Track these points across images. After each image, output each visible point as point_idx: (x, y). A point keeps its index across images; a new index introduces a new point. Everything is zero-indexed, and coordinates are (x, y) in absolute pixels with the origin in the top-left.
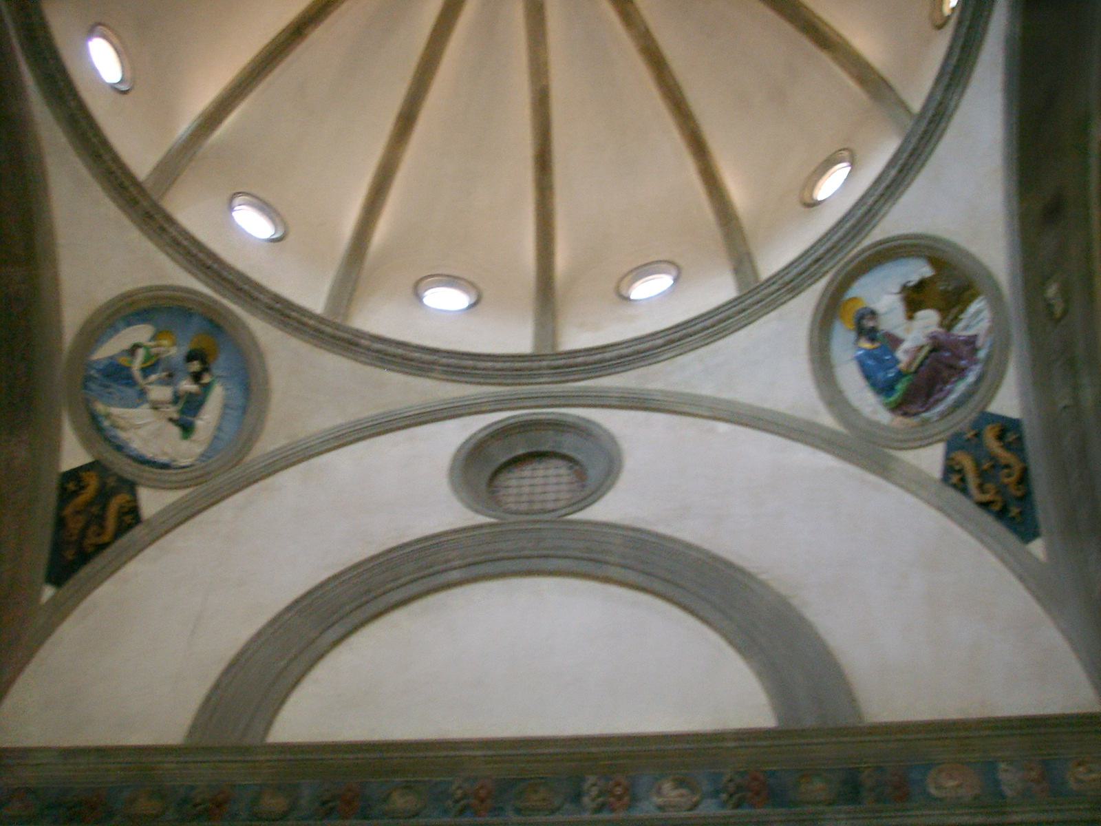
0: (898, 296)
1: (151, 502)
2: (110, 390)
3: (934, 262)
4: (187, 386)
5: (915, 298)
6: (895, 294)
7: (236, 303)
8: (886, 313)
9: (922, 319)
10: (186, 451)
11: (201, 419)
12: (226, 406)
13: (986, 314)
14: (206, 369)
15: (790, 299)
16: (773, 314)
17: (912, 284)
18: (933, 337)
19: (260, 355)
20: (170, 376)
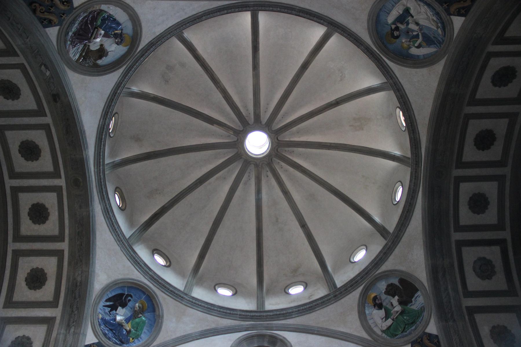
0: (108, 51)
3: (96, 66)
4: (402, 27)
5: (102, 52)
6: (109, 52)
7: (374, 50)
8: (112, 44)
11: (399, 13)
12: (389, 14)
13: (71, 55)
15: (151, 41)
16: (158, 34)
17: (104, 58)
18: (90, 42)
19: (369, 29)
20: (408, 32)
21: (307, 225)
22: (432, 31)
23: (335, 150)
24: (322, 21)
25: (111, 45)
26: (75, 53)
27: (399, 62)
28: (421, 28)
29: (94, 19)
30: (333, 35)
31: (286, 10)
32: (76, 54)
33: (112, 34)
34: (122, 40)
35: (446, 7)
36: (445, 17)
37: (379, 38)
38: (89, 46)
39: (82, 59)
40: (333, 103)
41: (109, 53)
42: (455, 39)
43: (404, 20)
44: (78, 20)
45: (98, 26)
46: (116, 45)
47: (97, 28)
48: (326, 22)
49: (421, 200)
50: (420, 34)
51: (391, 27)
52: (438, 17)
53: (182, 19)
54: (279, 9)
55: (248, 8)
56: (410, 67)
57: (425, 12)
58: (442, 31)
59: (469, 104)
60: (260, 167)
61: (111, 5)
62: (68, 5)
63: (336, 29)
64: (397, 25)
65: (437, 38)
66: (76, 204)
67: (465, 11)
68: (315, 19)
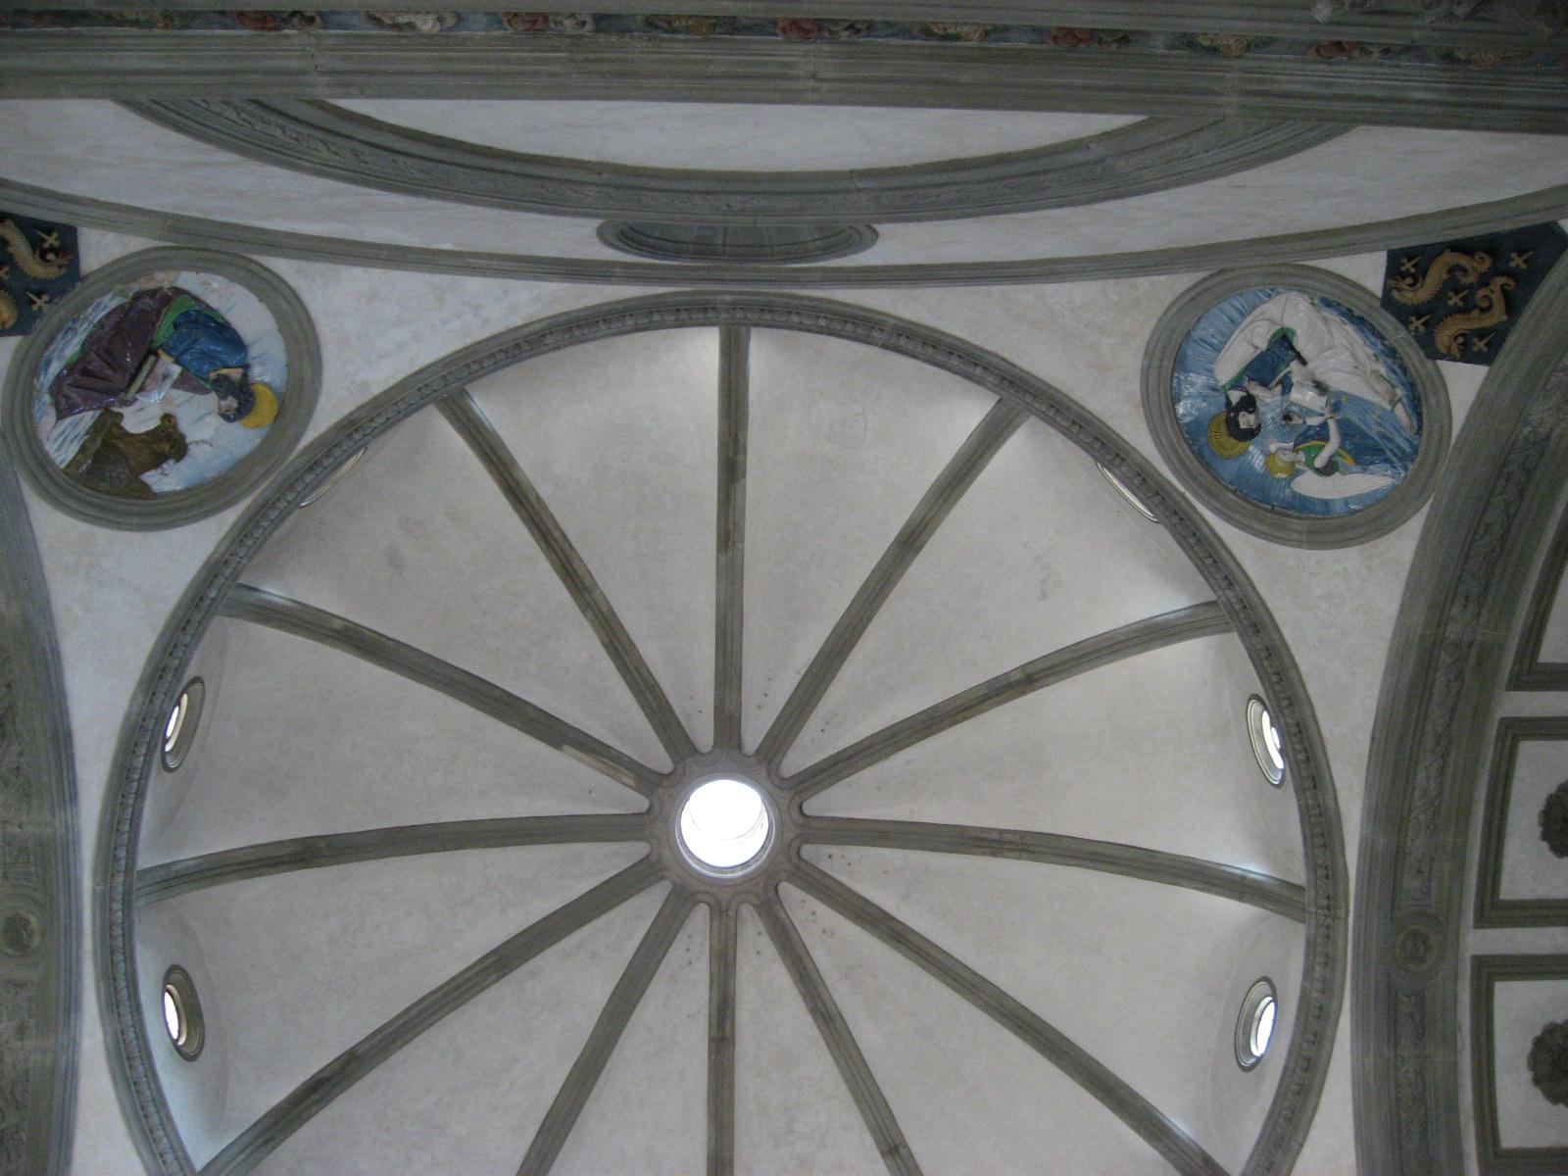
0: (188, 440)
1: (1368, 270)
2: (1379, 420)
3: (145, 491)
5: (168, 442)
6: (191, 443)
7: (1168, 481)
9: (154, 417)
10: (1294, 312)
14: (1232, 411)
16: (377, 390)
17: (171, 462)
19: (1146, 402)
21: (906, 1146)
22: (1374, 412)
23: (1020, 858)
24: (978, 371)
25: (200, 418)
26: (64, 441)
27: (1259, 527)
28: (1333, 401)
29: (150, 319)
30: (1017, 427)
31: (849, 327)
32: (68, 443)
33: (206, 380)
34: (239, 403)
35: (1422, 329)
36: (1418, 365)
37: (1185, 439)
38: (120, 416)
39: (89, 461)
40: (1012, 680)
41: (191, 446)
42: (1456, 443)
43: (1274, 372)
44: (91, 318)
45: (161, 346)
46: (214, 422)
47: (156, 354)
48: (992, 373)
49: (1348, 1045)
50: (1332, 424)
51: (1227, 397)
52: (1395, 363)
53: (469, 341)
54: (822, 322)
55: (711, 315)
56: (1299, 544)
57: (1347, 348)
58: (1408, 414)
59: (1516, 684)
60: (731, 914)
61: (215, 276)
62: (60, 261)
63: (1029, 398)
64: (1248, 392)
65: (1391, 440)
66: (5, 1017)
67: (1487, 344)
68: (954, 361)
